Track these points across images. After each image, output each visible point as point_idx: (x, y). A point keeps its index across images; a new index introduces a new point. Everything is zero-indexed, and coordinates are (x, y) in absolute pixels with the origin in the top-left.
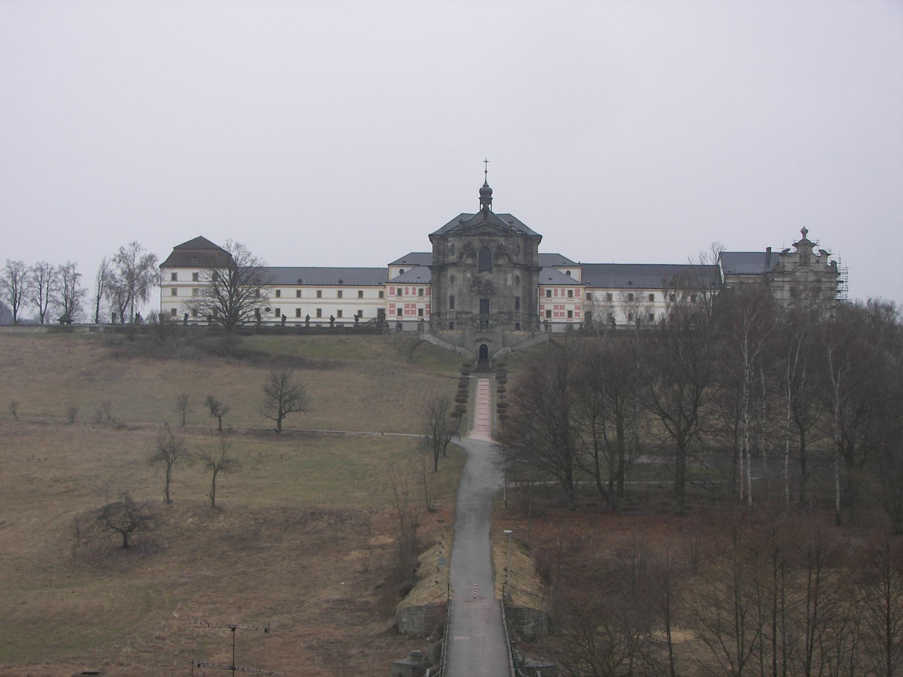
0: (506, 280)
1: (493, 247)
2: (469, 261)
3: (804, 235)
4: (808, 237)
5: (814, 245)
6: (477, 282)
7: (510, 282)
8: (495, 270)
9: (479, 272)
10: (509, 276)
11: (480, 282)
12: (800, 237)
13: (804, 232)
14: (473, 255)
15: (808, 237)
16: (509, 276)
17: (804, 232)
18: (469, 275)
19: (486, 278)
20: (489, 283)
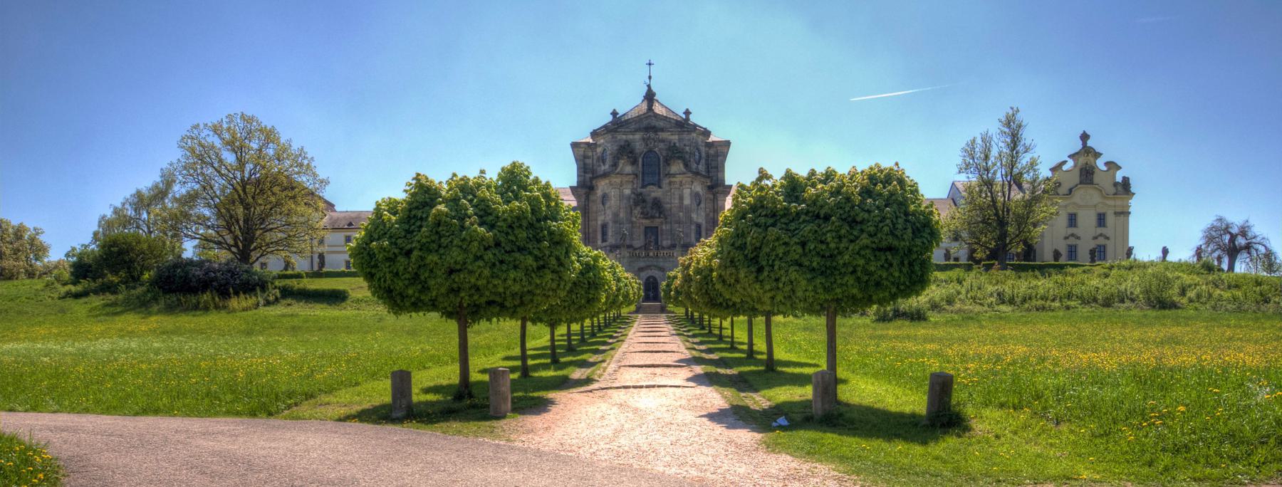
0: (681, 198)
1: (660, 148)
2: (629, 169)
3: (1084, 144)
4: (1090, 143)
5: (1097, 155)
6: (639, 200)
7: (687, 202)
8: (665, 181)
9: (644, 186)
10: (687, 192)
11: (644, 201)
12: (1078, 146)
13: (1085, 137)
14: (634, 162)
15: (1090, 143)
16: (687, 192)
17: (1085, 137)
18: (627, 192)
19: (653, 195)
20: (657, 204)
